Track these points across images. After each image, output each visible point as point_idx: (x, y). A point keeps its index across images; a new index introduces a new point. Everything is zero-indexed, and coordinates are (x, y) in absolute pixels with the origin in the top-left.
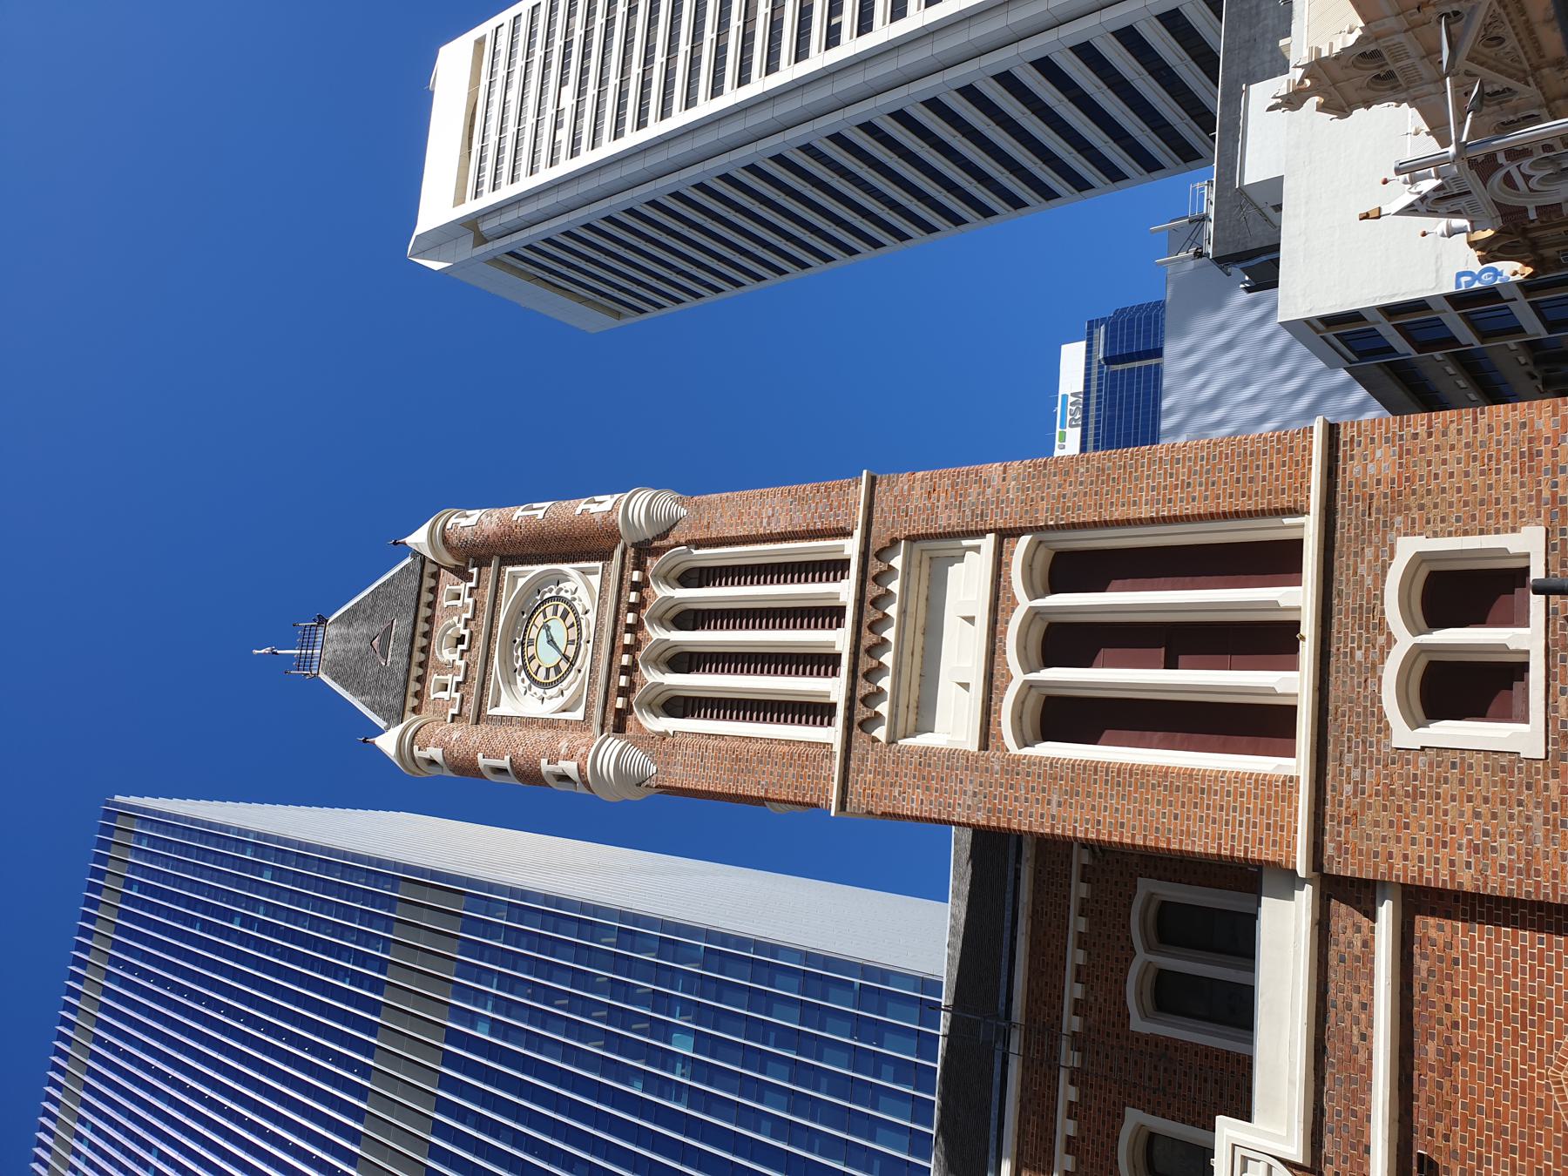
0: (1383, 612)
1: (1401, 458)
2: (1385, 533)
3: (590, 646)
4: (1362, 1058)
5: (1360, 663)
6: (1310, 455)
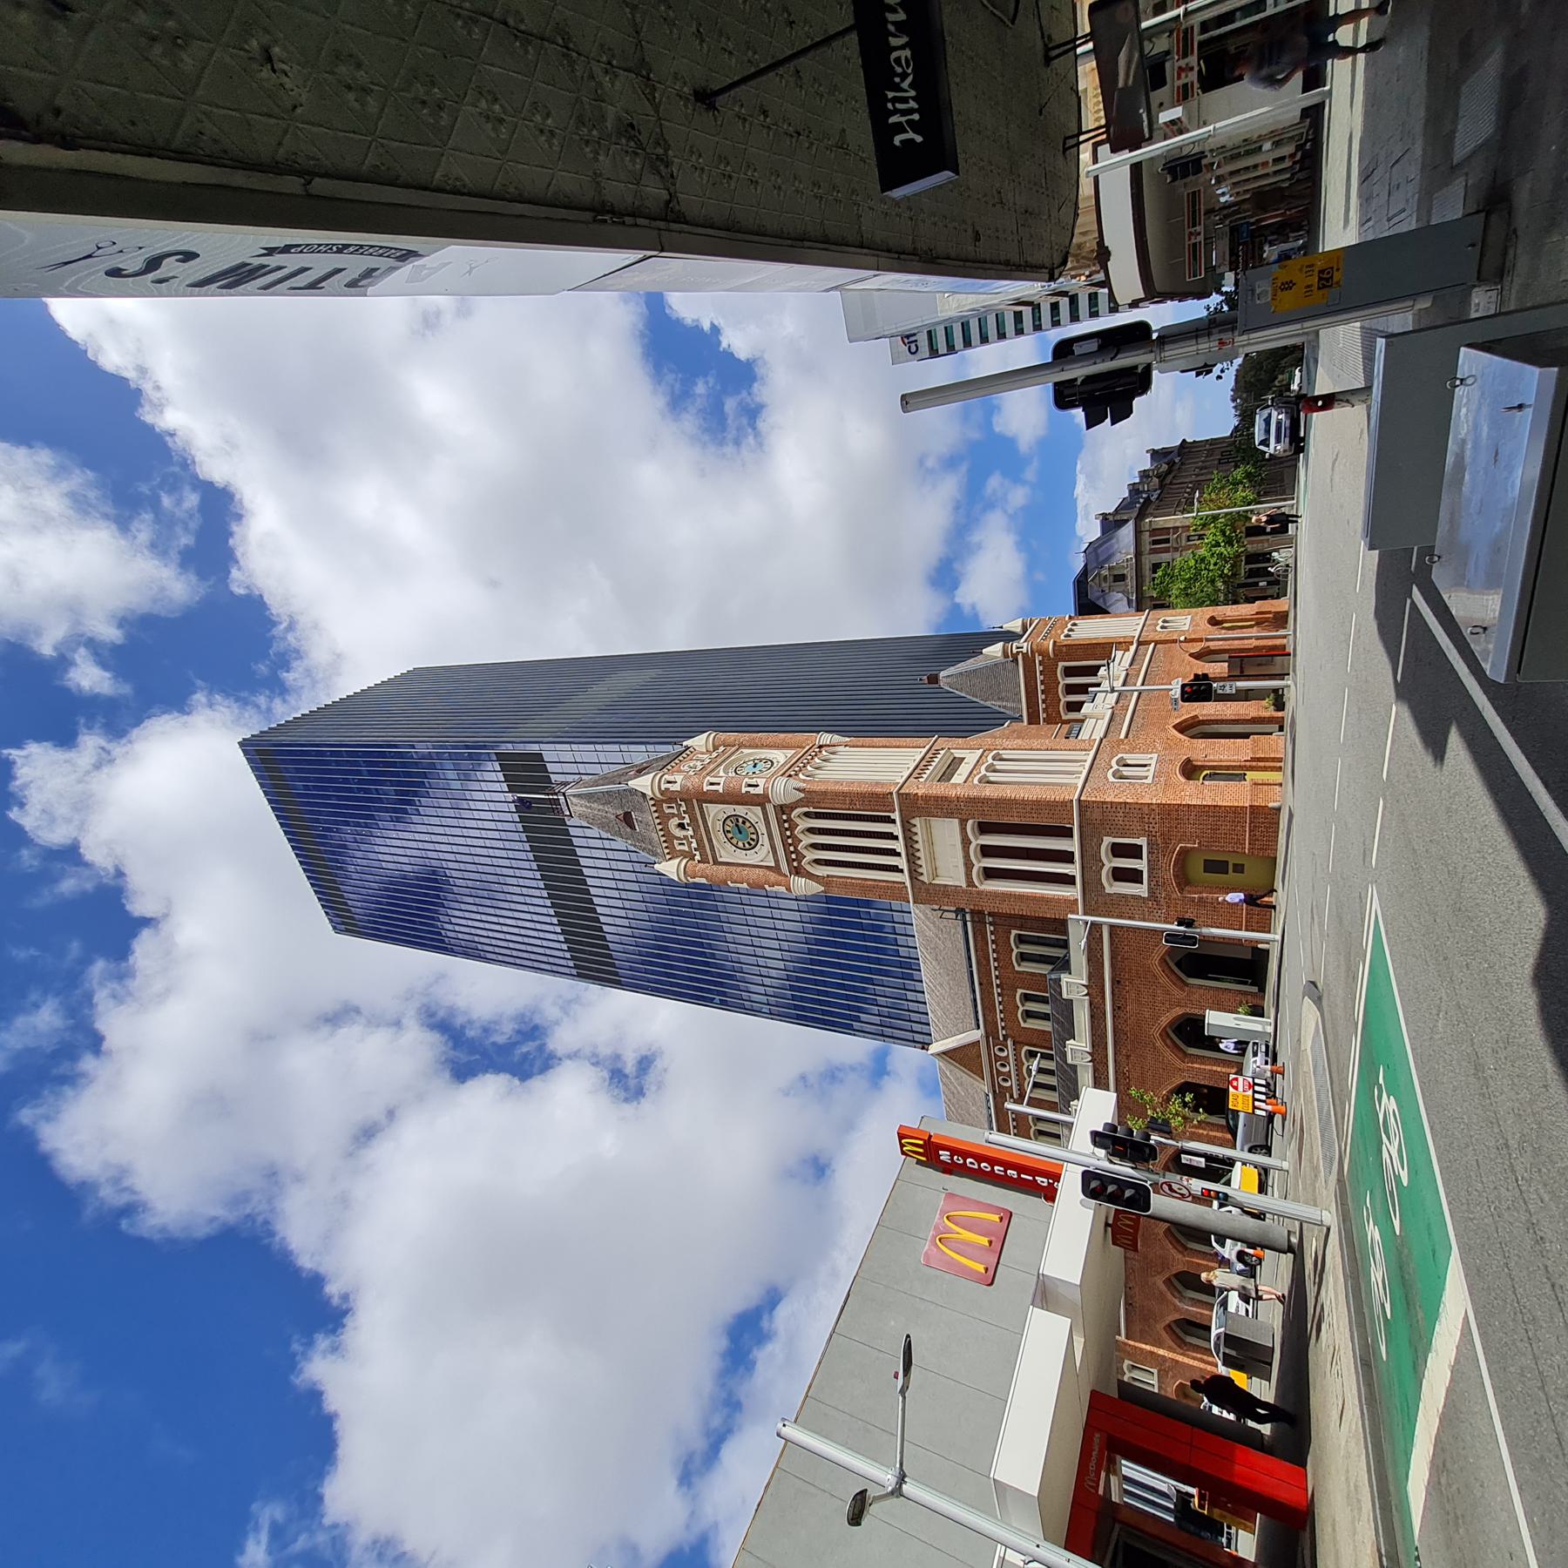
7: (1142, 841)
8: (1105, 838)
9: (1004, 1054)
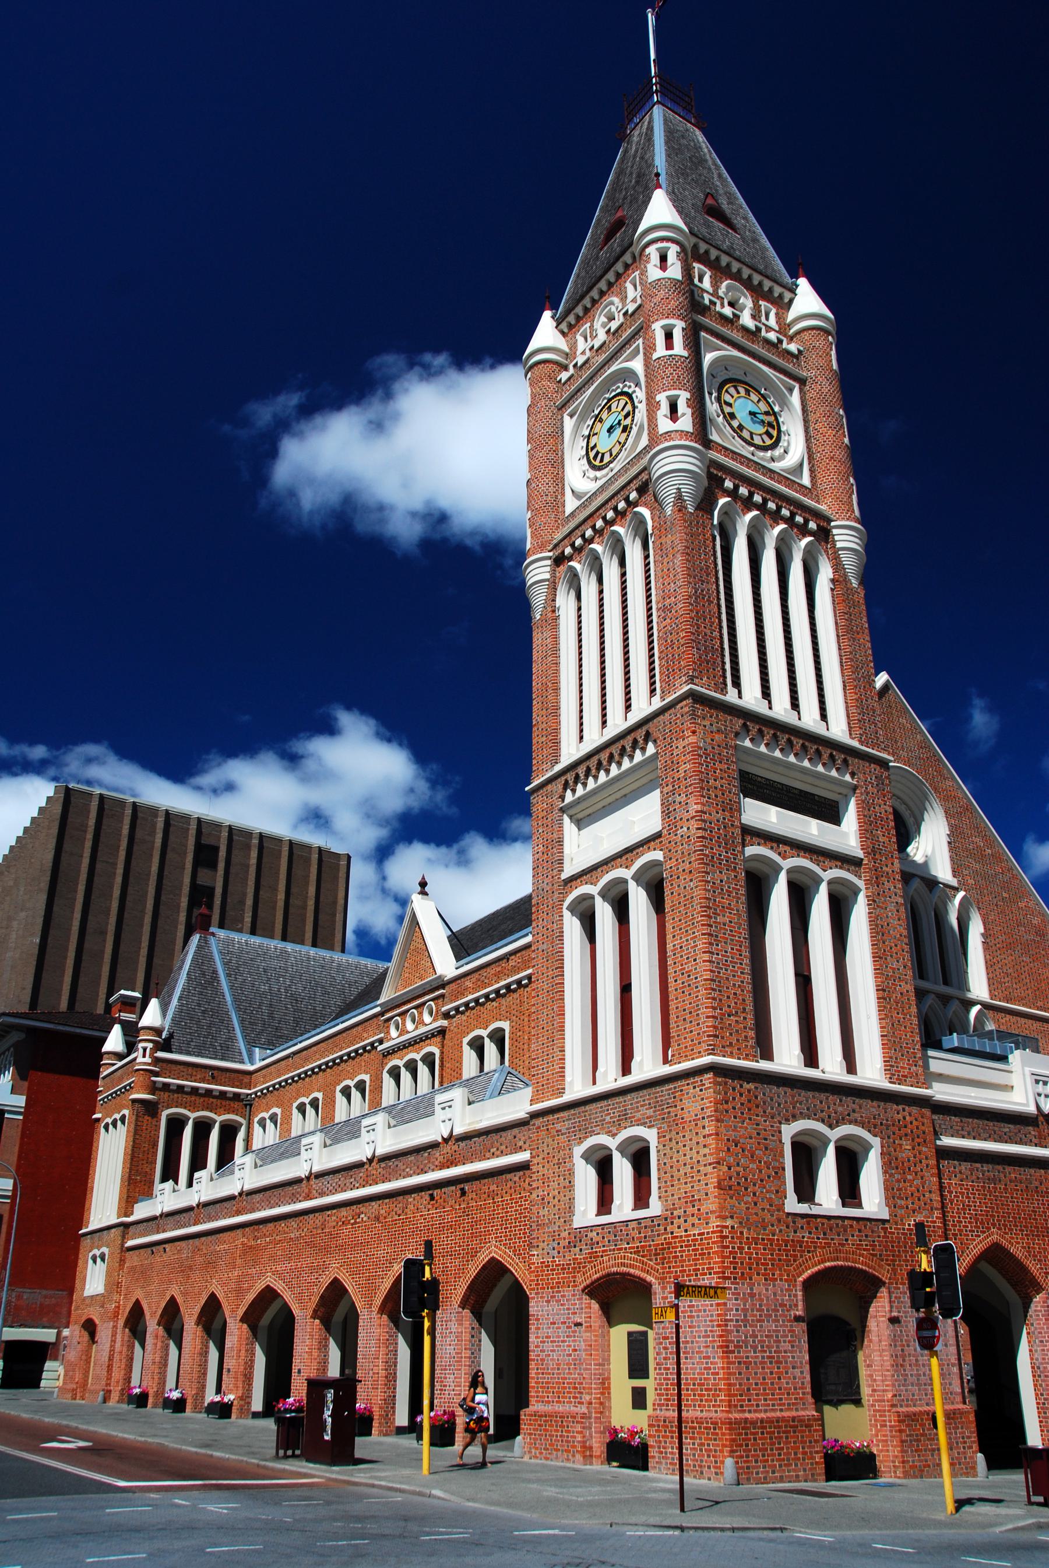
0: (625, 1128)
1: (694, 1120)
2: (659, 1120)
3: (611, 474)
4: (488, 1155)
5: (604, 1120)
6: (697, 1058)
7: (655, 1207)
8: (655, 1131)
9: (427, 1018)
